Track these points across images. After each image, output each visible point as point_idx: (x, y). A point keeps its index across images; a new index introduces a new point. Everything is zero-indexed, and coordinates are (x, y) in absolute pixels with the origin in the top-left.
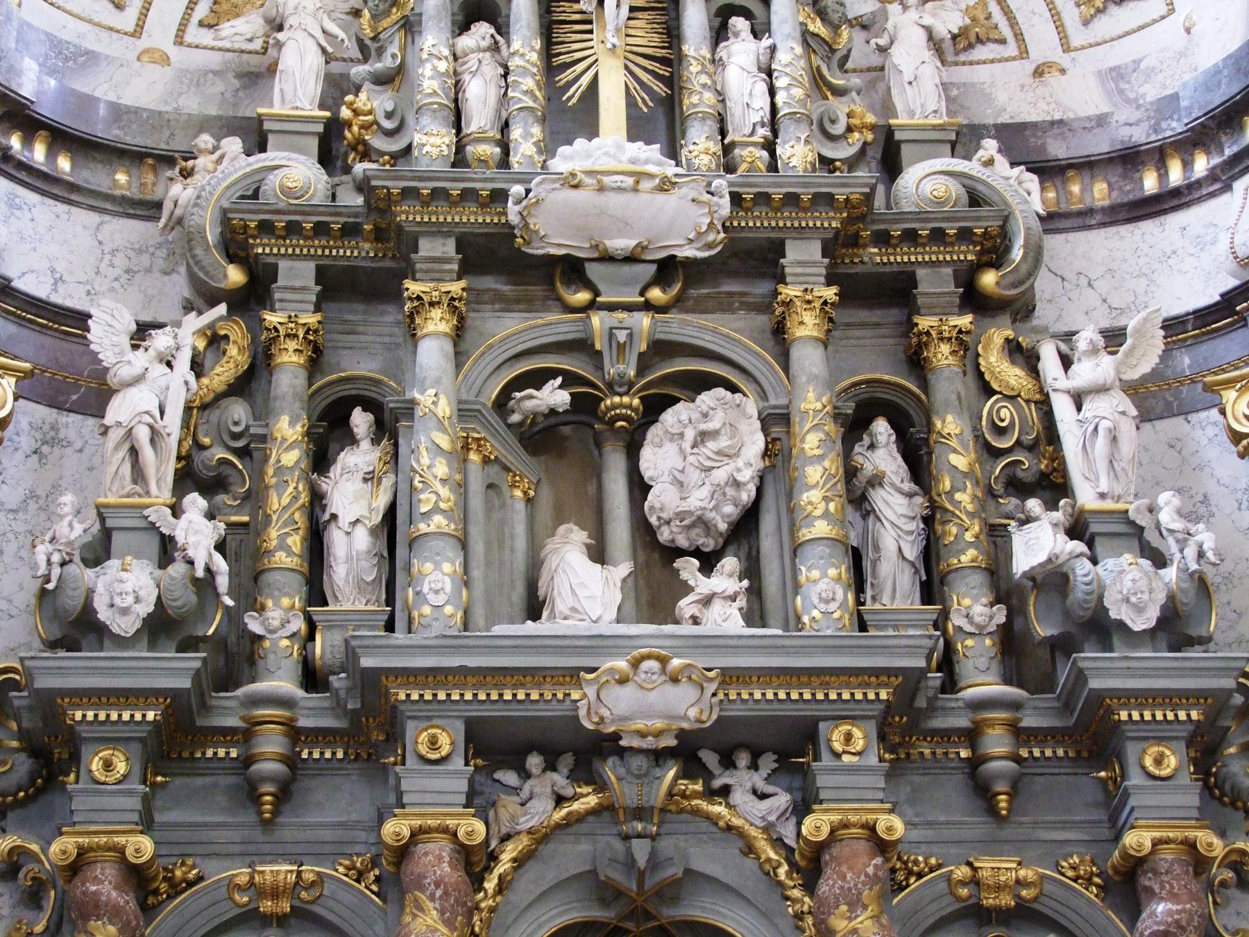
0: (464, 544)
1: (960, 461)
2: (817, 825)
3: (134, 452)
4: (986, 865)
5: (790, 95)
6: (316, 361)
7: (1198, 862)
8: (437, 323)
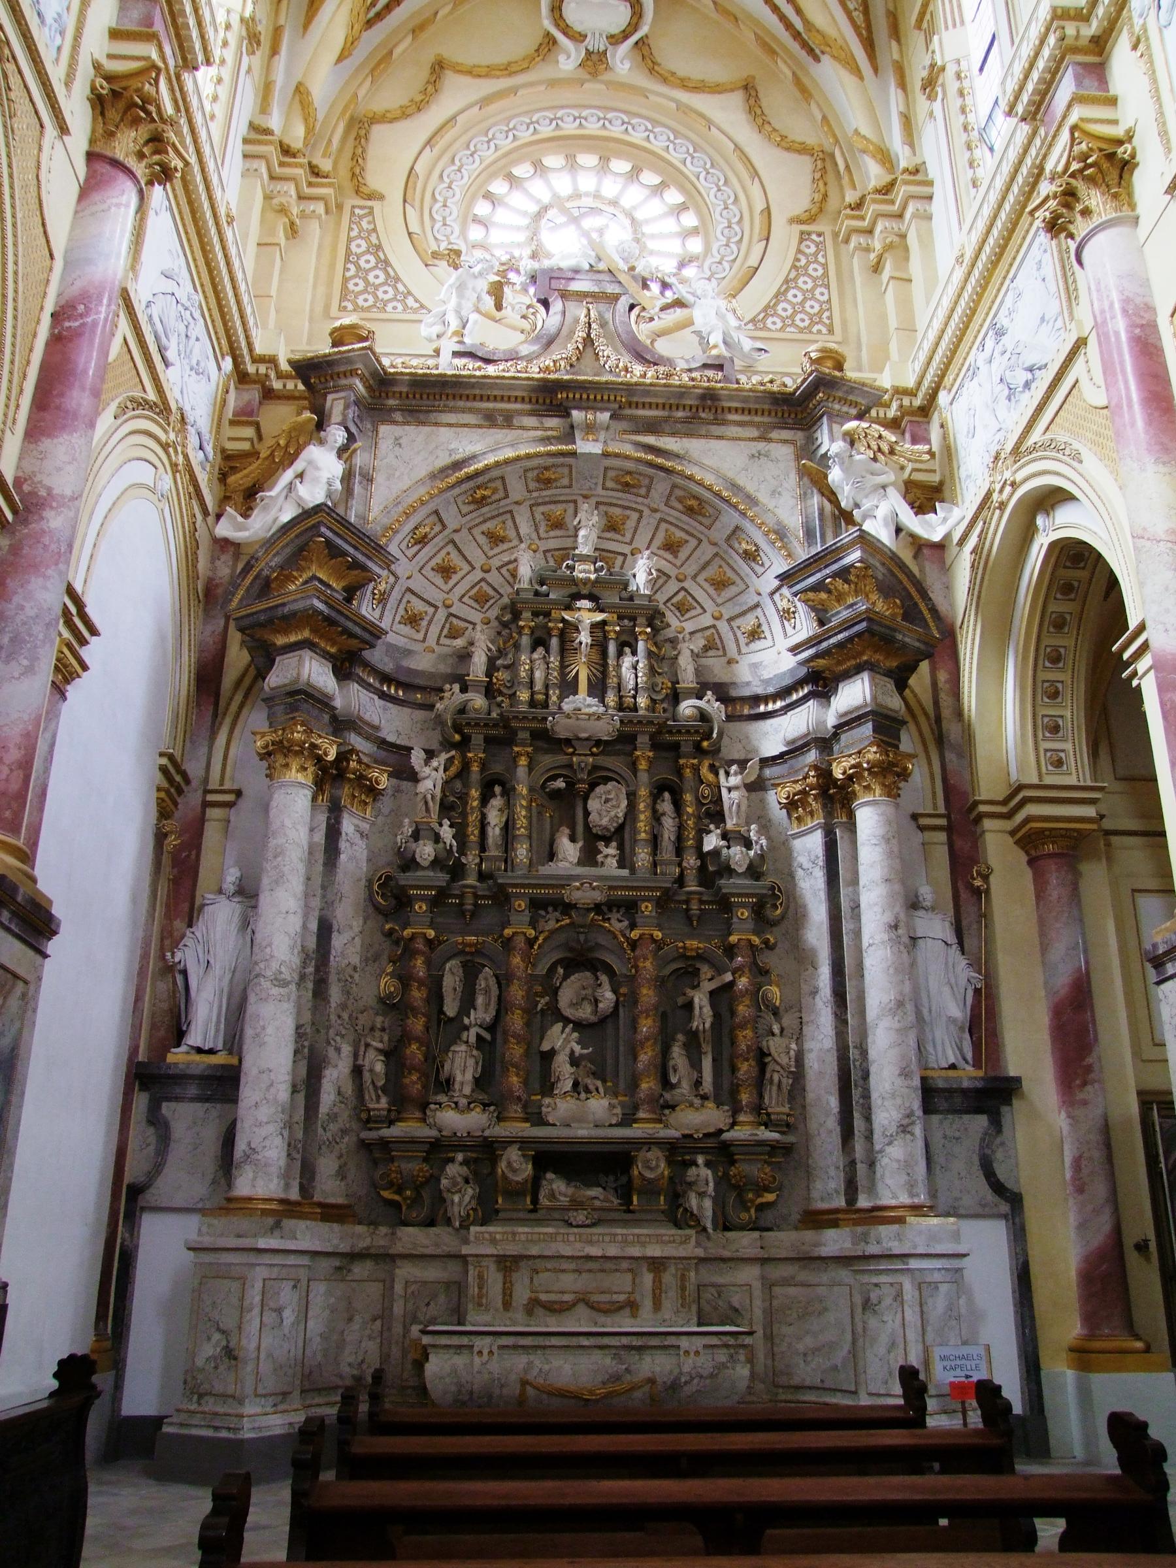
0: (530, 837)
1: (690, 810)
2: (635, 934)
3: (426, 803)
4: (688, 942)
6: (484, 766)
7: (752, 946)
8: (523, 761)
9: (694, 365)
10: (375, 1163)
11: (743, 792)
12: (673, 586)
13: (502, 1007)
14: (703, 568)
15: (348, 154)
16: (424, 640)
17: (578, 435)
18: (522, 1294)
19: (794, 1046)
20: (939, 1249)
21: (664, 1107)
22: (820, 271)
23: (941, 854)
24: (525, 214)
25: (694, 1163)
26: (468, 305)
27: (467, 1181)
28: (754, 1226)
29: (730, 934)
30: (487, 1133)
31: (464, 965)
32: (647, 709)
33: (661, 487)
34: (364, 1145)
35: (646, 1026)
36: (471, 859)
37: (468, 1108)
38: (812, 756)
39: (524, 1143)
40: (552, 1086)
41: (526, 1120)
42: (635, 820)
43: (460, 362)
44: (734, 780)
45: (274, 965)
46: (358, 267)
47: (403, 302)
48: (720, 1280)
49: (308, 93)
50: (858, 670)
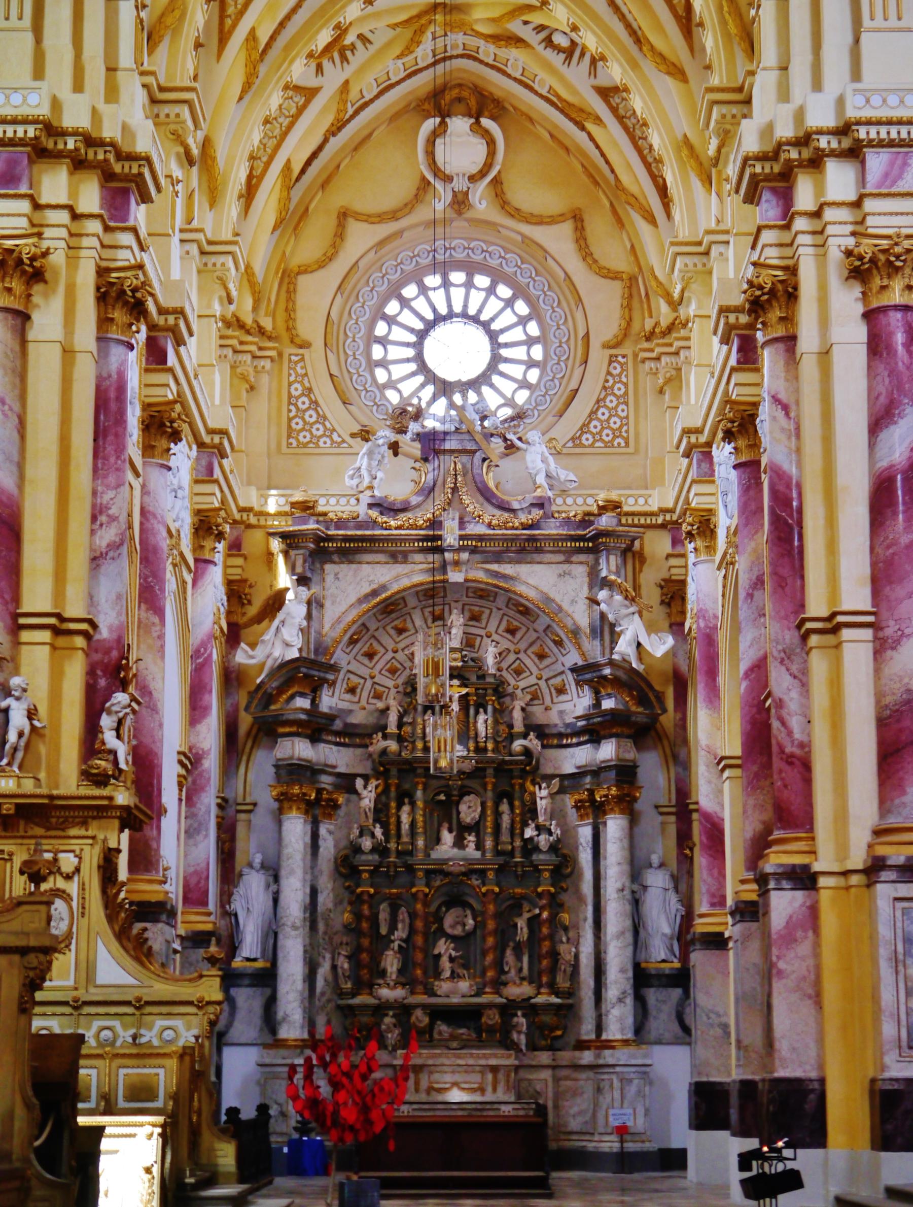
0: (425, 833)
2: (484, 890)
5: (490, 731)
6: (398, 786)
8: (420, 787)
9: (524, 505)
10: (346, 1016)
11: (548, 800)
12: (512, 657)
13: (412, 930)
14: (531, 645)
15: (282, 305)
16: (359, 702)
17: (449, 568)
18: (424, 1084)
19: (574, 950)
20: (633, 1062)
21: (498, 985)
22: (623, 390)
23: (672, 830)
24: (412, 330)
25: (516, 1015)
26: (375, 463)
27: (395, 1026)
28: (551, 1048)
29: (539, 885)
30: (406, 1001)
31: (390, 905)
32: (493, 751)
33: (501, 601)
34: (339, 1007)
35: (490, 941)
36: (392, 845)
37: (395, 987)
38: (588, 779)
39: (424, 1007)
40: (440, 974)
41: (425, 994)
42: (485, 820)
43: (374, 513)
44: (544, 793)
45: (292, 919)
46: (298, 409)
47: (330, 437)
48: (531, 1077)
49: (253, 274)
50: (611, 736)
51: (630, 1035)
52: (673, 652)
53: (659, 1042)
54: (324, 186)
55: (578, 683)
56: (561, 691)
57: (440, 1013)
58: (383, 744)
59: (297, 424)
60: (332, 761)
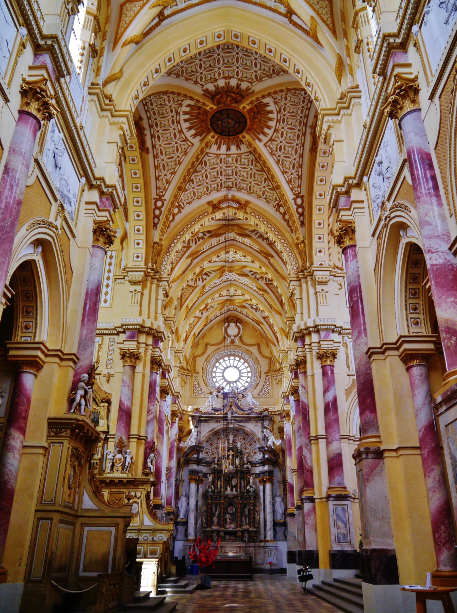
13: (220, 512)
18: (223, 551)
21: (241, 526)
23: (282, 487)
33: (241, 432)
34: (203, 531)
36: (216, 490)
39: (223, 531)
43: (213, 411)
51: (272, 539)
52: (281, 444)
53: (280, 540)
54: (203, 338)
55: (259, 451)
56: (255, 453)
57: (227, 533)
58: (214, 466)
59: (196, 391)
60: (202, 470)
